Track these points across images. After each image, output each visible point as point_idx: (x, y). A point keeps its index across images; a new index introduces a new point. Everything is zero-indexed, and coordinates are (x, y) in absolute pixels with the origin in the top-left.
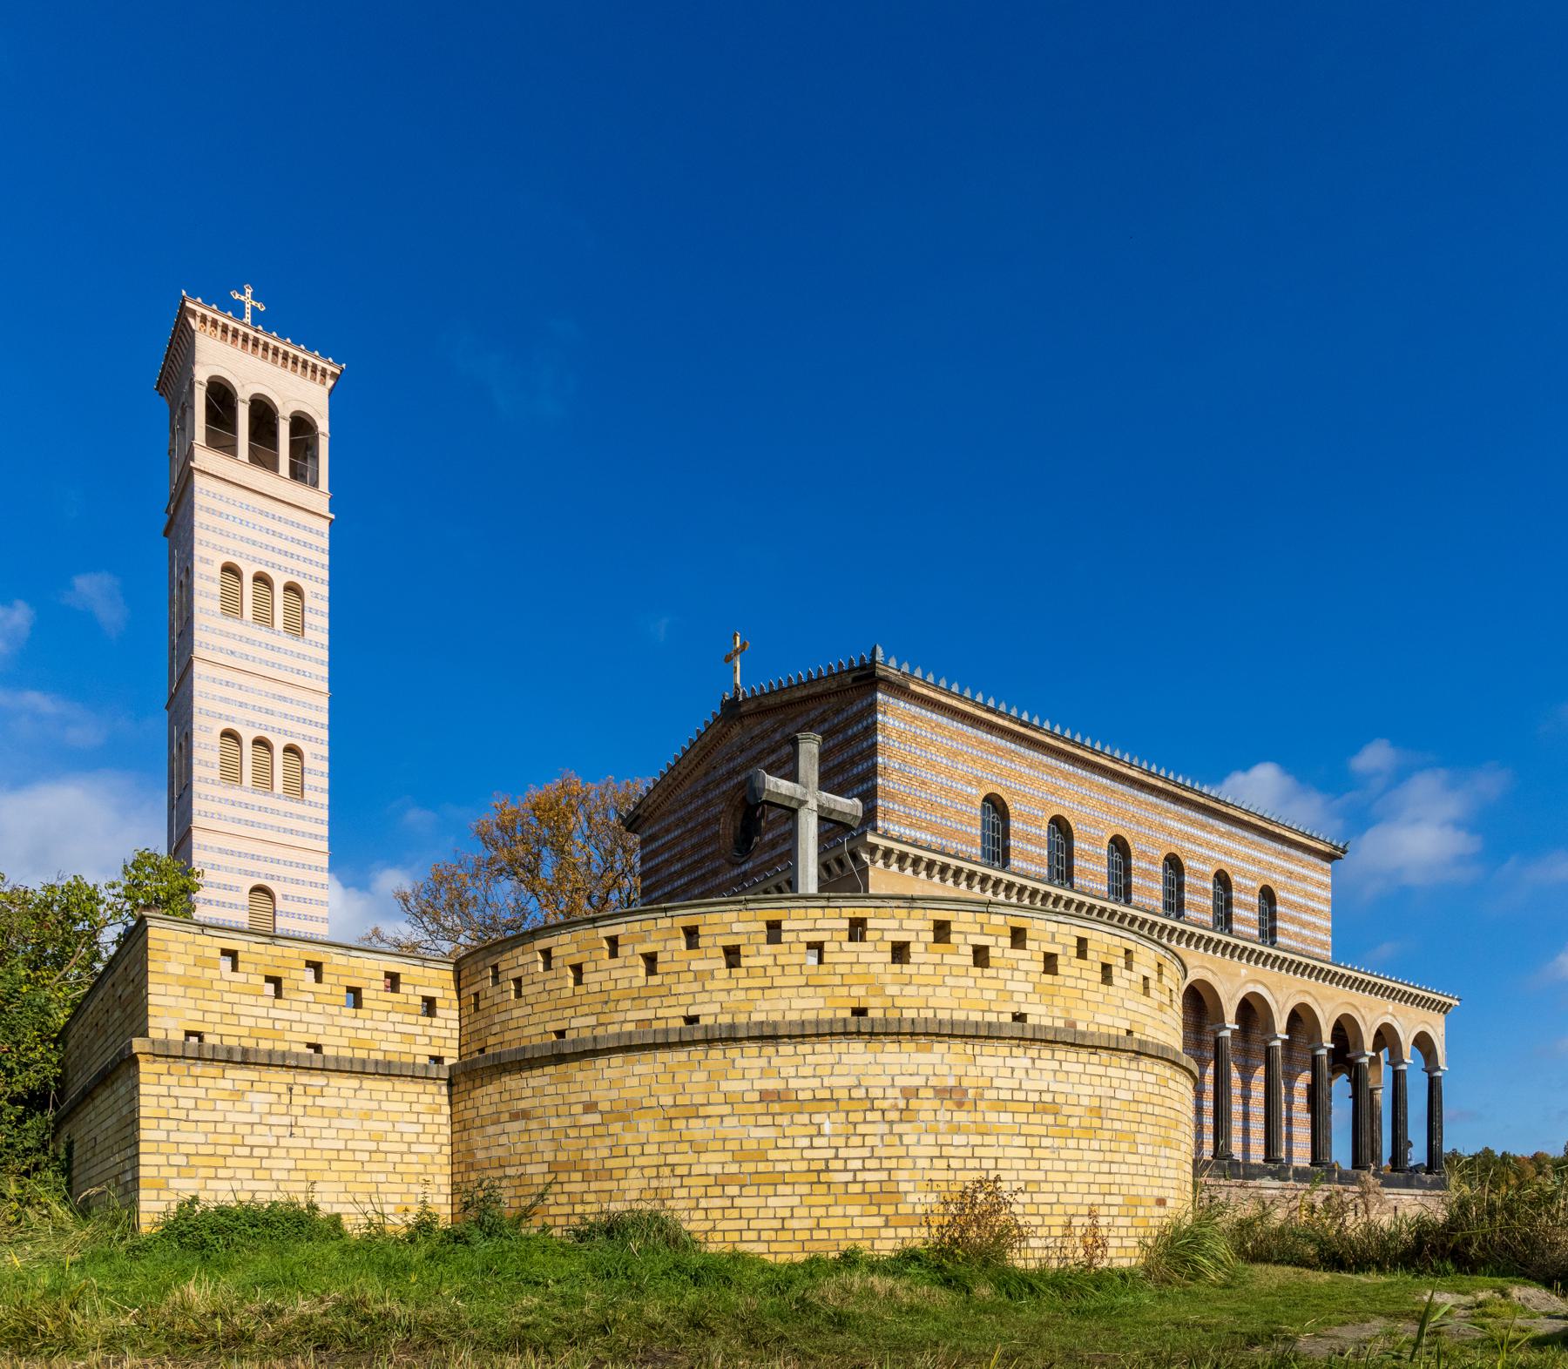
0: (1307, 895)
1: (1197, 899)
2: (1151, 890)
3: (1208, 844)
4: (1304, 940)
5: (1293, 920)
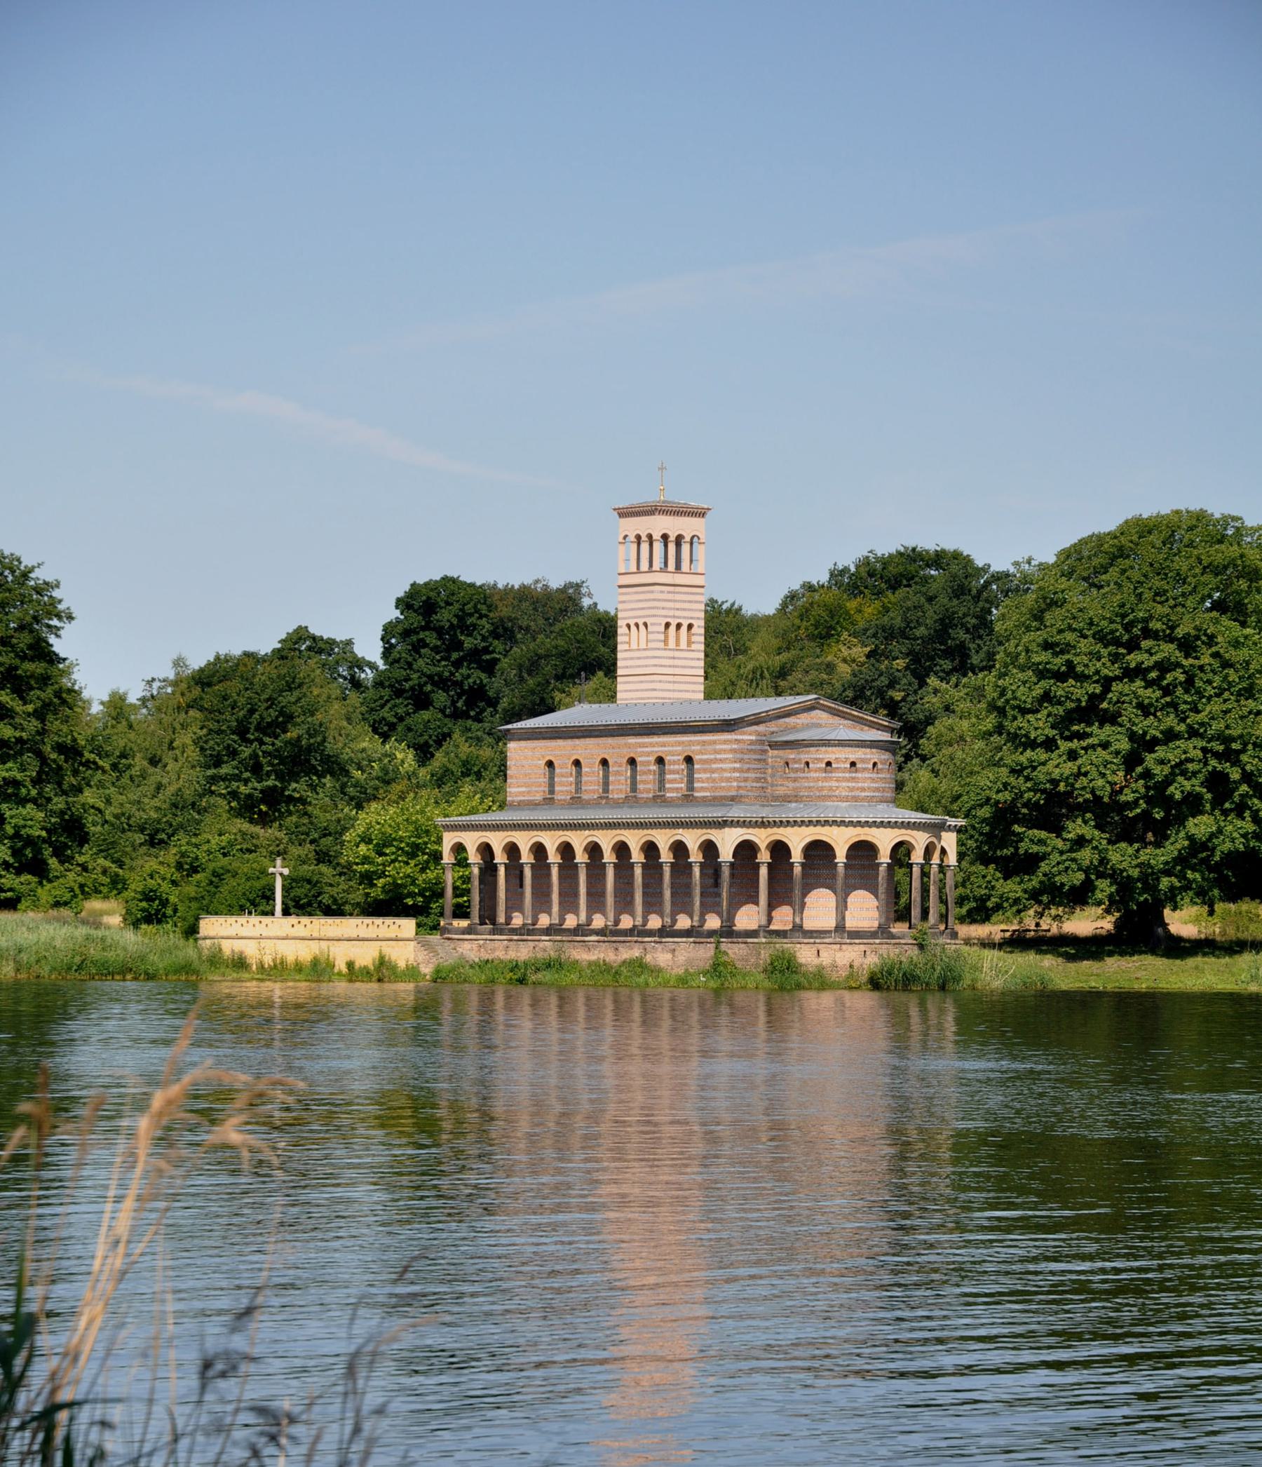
0: (716, 752)
1: (644, 777)
2: (619, 781)
3: (652, 745)
4: (714, 780)
5: (705, 771)
